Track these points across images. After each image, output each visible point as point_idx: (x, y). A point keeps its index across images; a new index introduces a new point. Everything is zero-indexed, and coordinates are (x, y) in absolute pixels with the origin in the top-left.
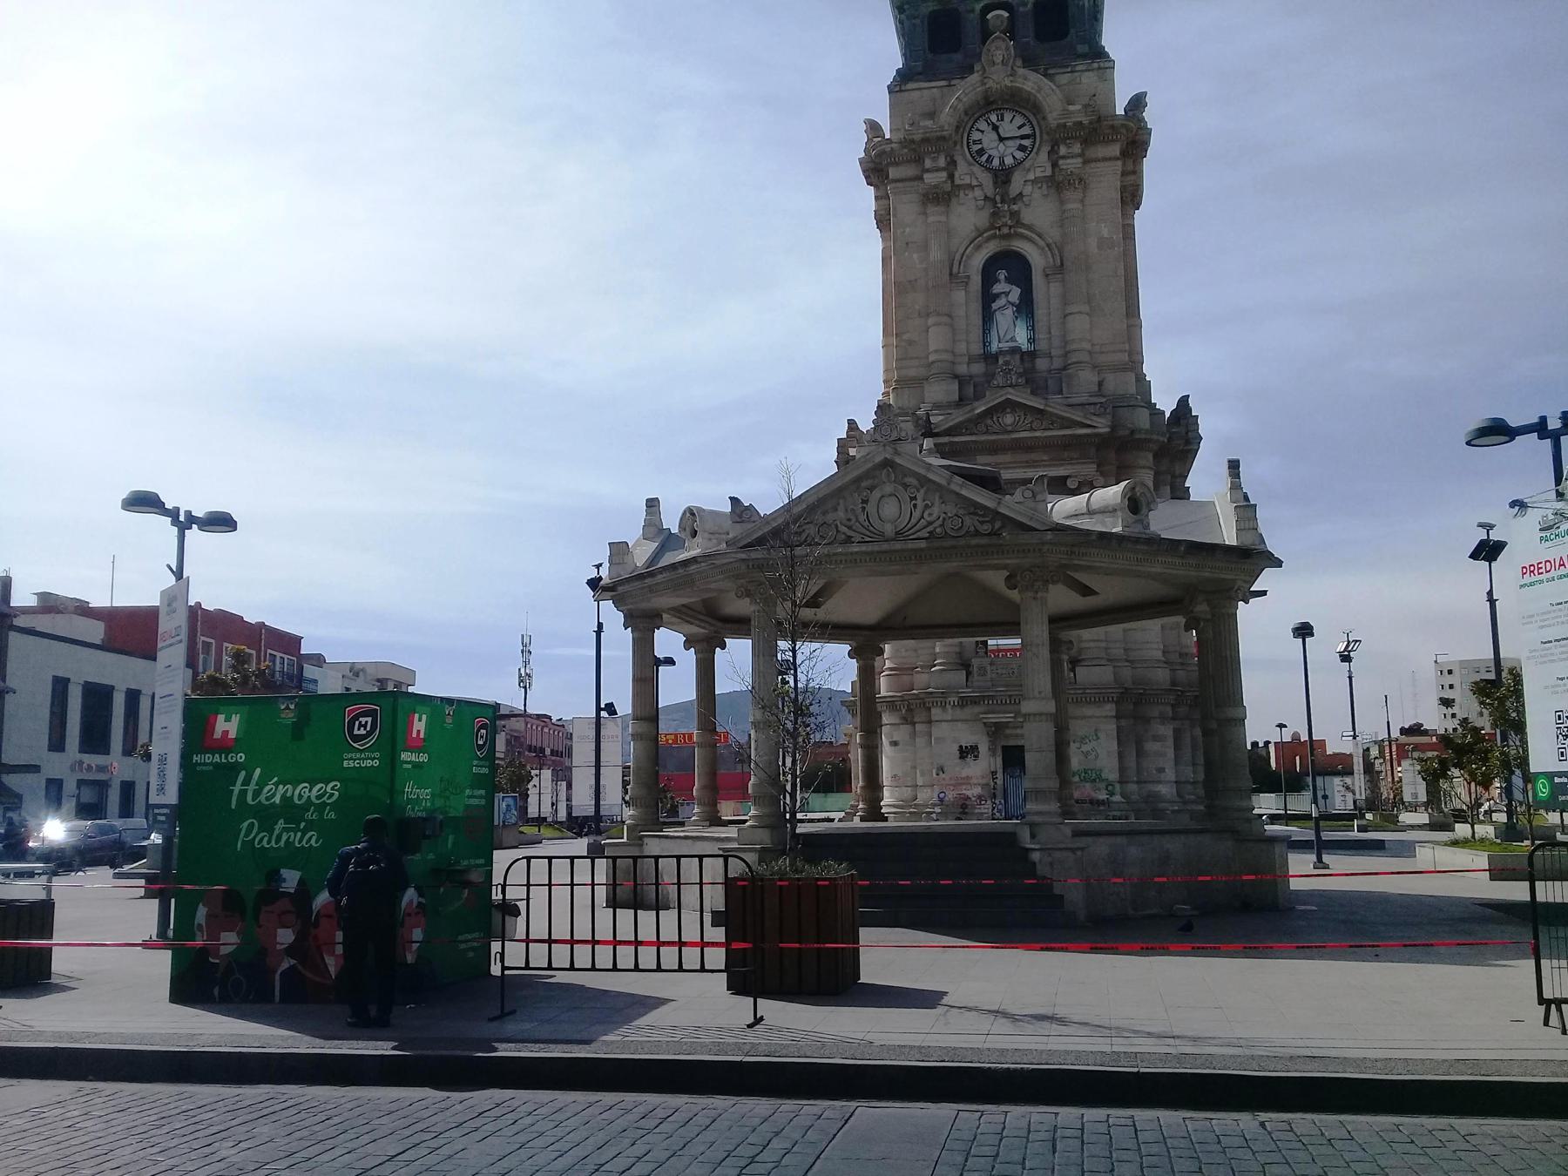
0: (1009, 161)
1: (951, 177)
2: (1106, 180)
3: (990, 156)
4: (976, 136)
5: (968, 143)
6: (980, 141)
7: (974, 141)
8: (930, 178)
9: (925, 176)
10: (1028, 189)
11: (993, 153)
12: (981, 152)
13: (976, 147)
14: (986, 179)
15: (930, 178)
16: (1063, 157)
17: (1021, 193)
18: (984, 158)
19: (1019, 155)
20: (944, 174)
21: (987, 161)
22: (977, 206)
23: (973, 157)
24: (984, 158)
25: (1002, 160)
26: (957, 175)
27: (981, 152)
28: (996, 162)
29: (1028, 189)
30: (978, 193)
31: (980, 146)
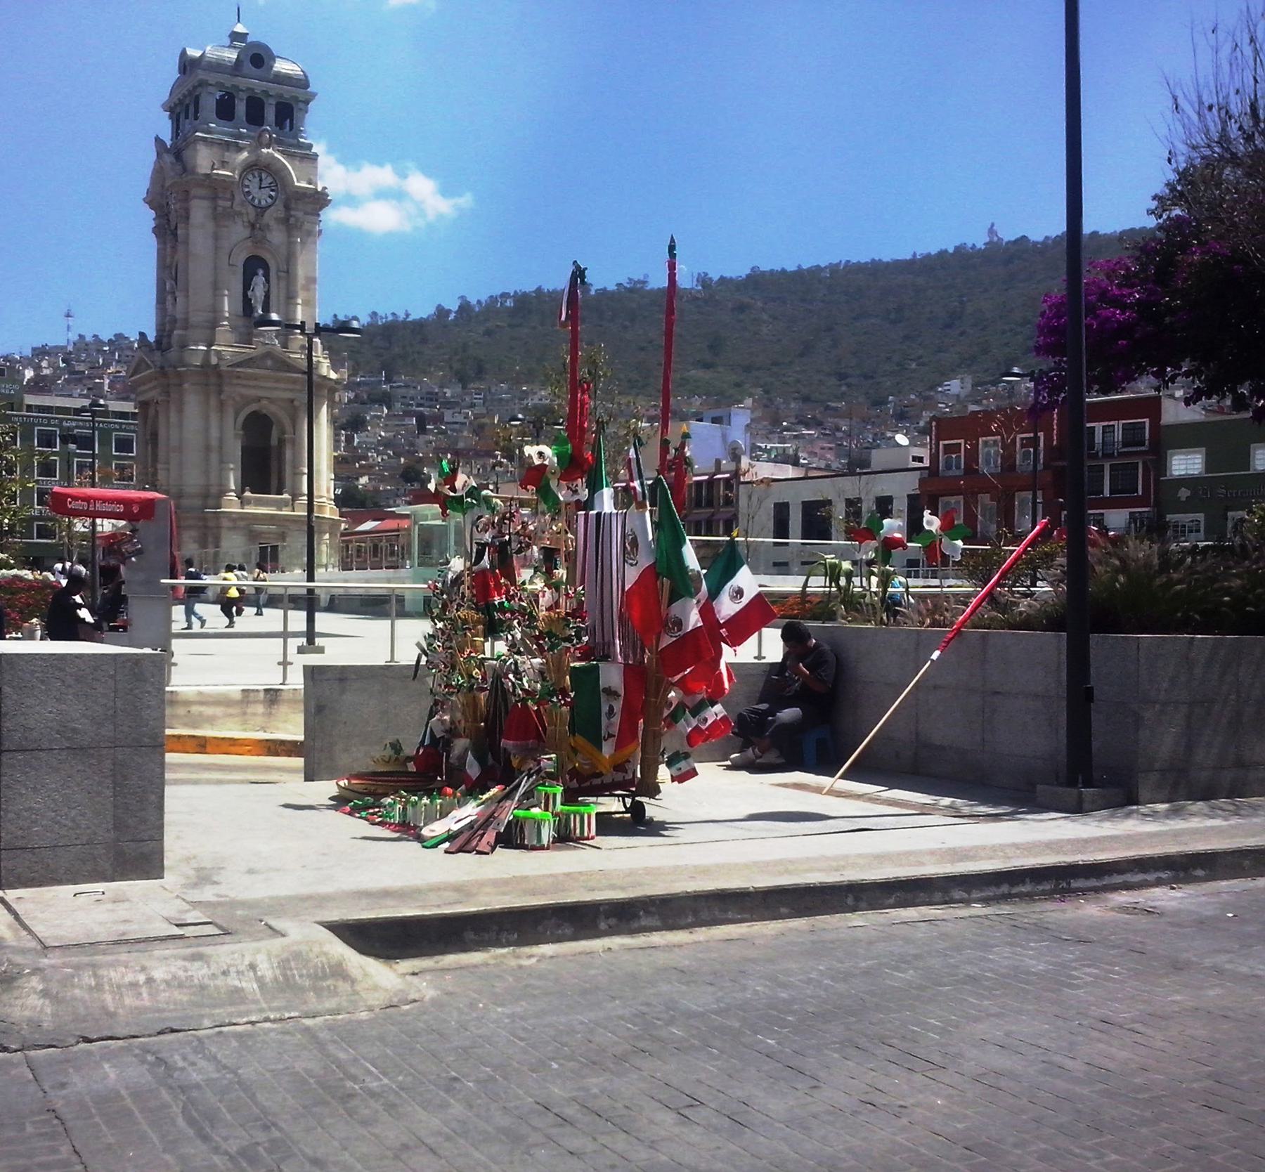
0: (263, 203)
6: (248, 186)
13: (247, 190)
14: (251, 209)
19: (269, 200)
25: (260, 202)
27: (249, 193)
28: (256, 201)
29: (272, 223)
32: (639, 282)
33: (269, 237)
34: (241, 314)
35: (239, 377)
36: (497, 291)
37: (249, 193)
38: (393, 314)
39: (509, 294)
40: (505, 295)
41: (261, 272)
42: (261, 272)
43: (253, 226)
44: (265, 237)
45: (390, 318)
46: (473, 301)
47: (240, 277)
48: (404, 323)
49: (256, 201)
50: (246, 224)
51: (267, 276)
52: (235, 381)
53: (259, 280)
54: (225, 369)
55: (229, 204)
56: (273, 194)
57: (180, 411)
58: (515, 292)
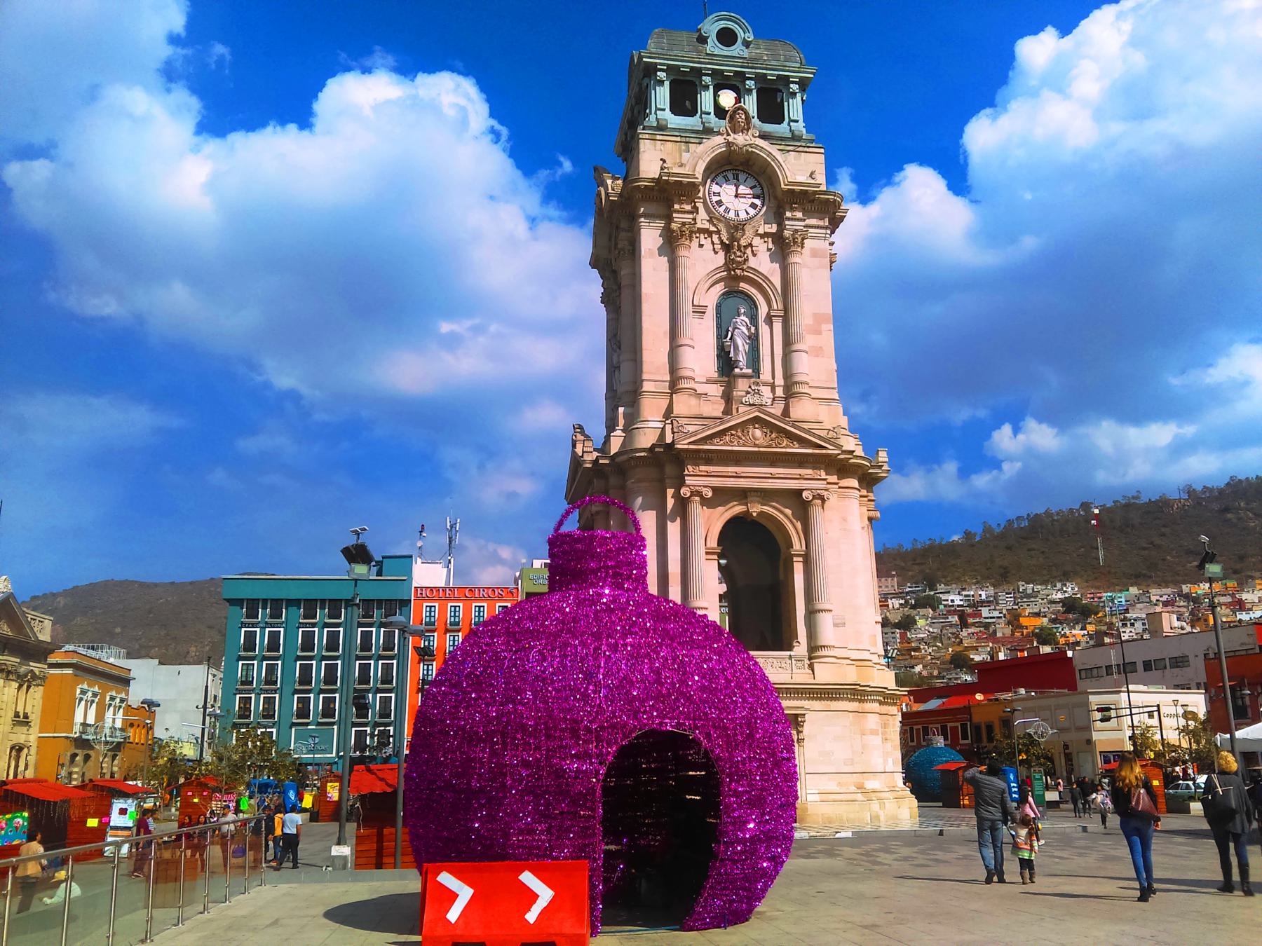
0: (743, 216)
5: (709, 194)
6: (719, 194)
7: (714, 193)
9: (675, 215)
10: (757, 241)
11: (729, 206)
13: (715, 199)
16: (789, 219)
18: (722, 209)
19: (752, 212)
21: (725, 211)
22: (714, 249)
23: (713, 207)
25: (737, 214)
26: (698, 221)
31: (718, 198)
32: (1134, 498)
33: (752, 262)
34: (716, 375)
35: (709, 462)
36: (1011, 515)
37: (720, 203)
38: (930, 539)
39: (1023, 517)
40: (1018, 518)
43: (727, 248)
44: (746, 260)
45: (928, 543)
46: (994, 526)
48: (940, 544)
50: (718, 247)
51: (754, 319)
54: (686, 447)
55: (687, 218)
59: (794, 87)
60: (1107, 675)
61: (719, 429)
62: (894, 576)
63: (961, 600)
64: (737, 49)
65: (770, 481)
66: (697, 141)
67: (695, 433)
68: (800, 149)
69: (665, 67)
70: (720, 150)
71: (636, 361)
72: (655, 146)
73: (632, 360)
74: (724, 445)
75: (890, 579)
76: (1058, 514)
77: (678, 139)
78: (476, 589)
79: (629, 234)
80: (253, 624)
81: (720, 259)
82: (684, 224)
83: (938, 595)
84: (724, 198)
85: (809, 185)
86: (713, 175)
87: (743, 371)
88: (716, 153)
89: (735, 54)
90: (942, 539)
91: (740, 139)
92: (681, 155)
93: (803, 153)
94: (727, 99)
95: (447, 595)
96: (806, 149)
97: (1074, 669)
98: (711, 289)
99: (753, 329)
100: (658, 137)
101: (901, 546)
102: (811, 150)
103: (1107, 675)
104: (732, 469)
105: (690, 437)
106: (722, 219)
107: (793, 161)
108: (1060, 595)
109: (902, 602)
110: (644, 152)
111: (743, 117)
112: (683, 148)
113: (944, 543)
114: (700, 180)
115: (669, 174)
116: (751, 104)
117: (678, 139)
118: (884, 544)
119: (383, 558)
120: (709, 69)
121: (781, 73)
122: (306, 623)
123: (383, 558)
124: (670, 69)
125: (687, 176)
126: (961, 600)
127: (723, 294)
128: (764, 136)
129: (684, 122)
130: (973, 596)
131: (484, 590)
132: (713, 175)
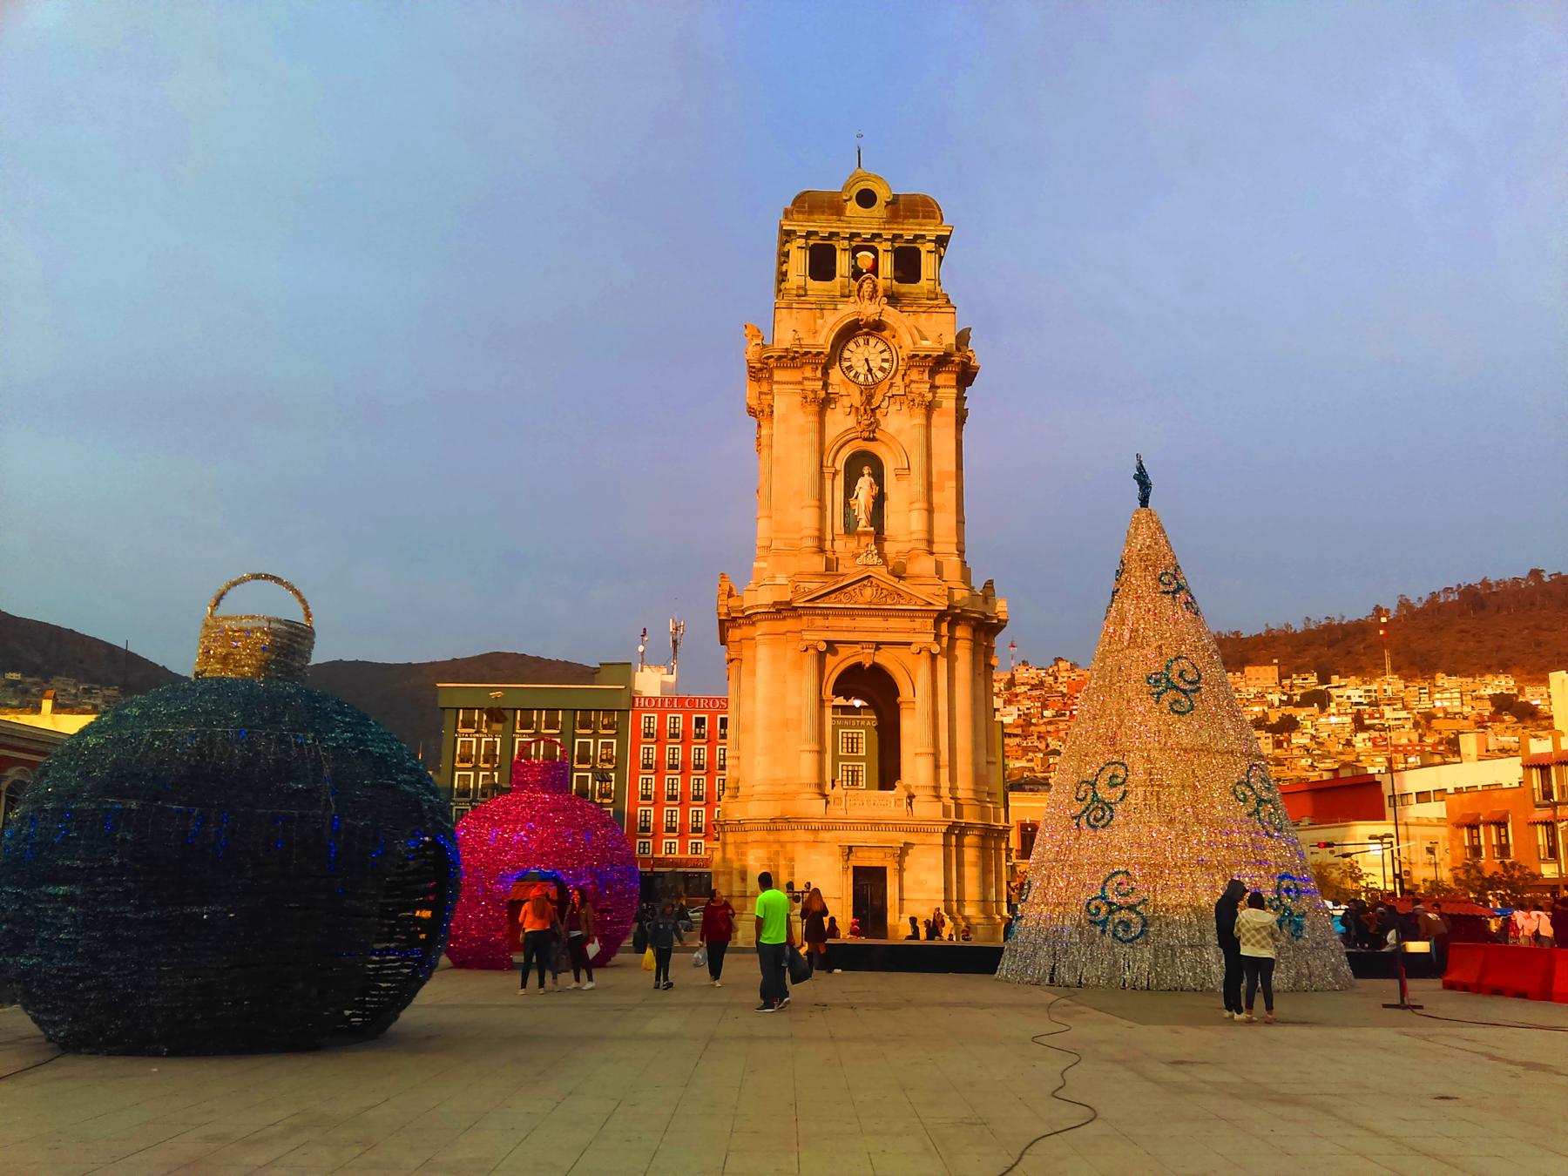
1: (826, 385)
2: (947, 398)
3: (857, 373)
4: (846, 354)
8: (809, 385)
12: (850, 368)
15: (809, 385)
17: (879, 406)
18: (852, 374)
20: (821, 383)
21: (854, 377)
24: (852, 374)
27: (850, 368)
28: (861, 378)
30: (846, 402)
31: (849, 364)
35: (826, 616)
36: (1438, 587)
39: (1451, 589)
40: (1446, 589)
41: (866, 470)
42: (866, 470)
45: (1324, 622)
46: (1413, 600)
47: (840, 481)
48: (1340, 624)
49: (861, 378)
51: (878, 477)
52: (819, 622)
53: (864, 485)
56: (886, 365)
57: (753, 673)
58: (1459, 586)
59: (931, 246)
60: (1417, 802)
61: (833, 588)
62: (1275, 664)
63: (1360, 697)
64: (879, 210)
65: (881, 634)
66: (832, 307)
67: (811, 592)
68: (930, 310)
69: (805, 234)
70: (848, 320)
71: (771, 517)
72: (791, 314)
73: (767, 517)
74: (840, 602)
75: (1269, 669)
76: (1498, 584)
77: (814, 306)
78: (697, 700)
79: (769, 397)
80: (469, 734)
81: (851, 422)
82: (813, 391)
83: (1329, 690)
84: (853, 363)
85: (933, 350)
86: (845, 342)
87: (866, 529)
88: (845, 322)
89: (876, 214)
90: (1343, 618)
91: (870, 310)
92: (815, 322)
93: (934, 314)
94: (865, 258)
95: (666, 706)
96: (937, 310)
97: (1383, 796)
98: (842, 450)
99: (876, 489)
100: (795, 305)
101: (1288, 626)
102: (943, 310)
103: (1417, 802)
104: (845, 622)
105: (806, 596)
106: (853, 384)
107: (924, 322)
108: (1490, 691)
109: (1285, 698)
110: (780, 321)
111: (872, 286)
112: (818, 315)
113: (1344, 623)
114: (829, 350)
115: (801, 346)
116: (886, 265)
117: (814, 306)
118: (1267, 625)
119: (600, 664)
120: (846, 233)
121: (918, 233)
122: (523, 734)
123: (600, 664)
124: (809, 234)
125: (814, 346)
126: (1360, 697)
127: (852, 454)
128: (893, 299)
129: (821, 287)
130: (1375, 691)
131: (704, 701)
132: (845, 342)
